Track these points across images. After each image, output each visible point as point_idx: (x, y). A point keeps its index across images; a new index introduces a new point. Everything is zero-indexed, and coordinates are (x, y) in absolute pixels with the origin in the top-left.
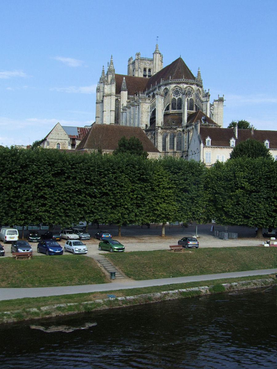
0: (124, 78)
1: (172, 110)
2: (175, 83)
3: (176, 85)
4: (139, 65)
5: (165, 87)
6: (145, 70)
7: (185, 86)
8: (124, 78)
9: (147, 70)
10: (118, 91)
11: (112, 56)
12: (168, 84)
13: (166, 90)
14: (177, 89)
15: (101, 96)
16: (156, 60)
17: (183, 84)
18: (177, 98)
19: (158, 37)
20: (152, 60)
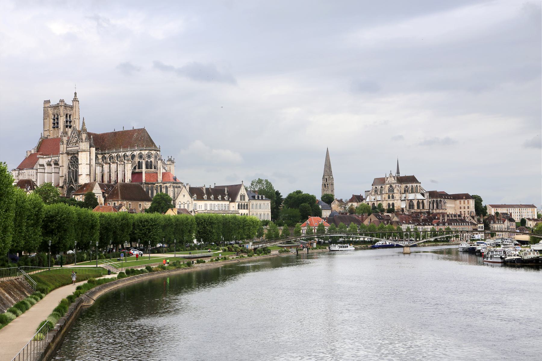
0: (92, 137)
1: (147, 170)
2: (148, 150)
4: (64, 111)
5: (140, 152)
6: (67, 115)
7: (155, 152)
8: (92, 137)
9: (68, 116)
10: (90, 147)
13: (141, 154)
14: (149, 154)
16: (76, 107)
17: (154, 151)
18: (149, 161)
20: (72, 107)
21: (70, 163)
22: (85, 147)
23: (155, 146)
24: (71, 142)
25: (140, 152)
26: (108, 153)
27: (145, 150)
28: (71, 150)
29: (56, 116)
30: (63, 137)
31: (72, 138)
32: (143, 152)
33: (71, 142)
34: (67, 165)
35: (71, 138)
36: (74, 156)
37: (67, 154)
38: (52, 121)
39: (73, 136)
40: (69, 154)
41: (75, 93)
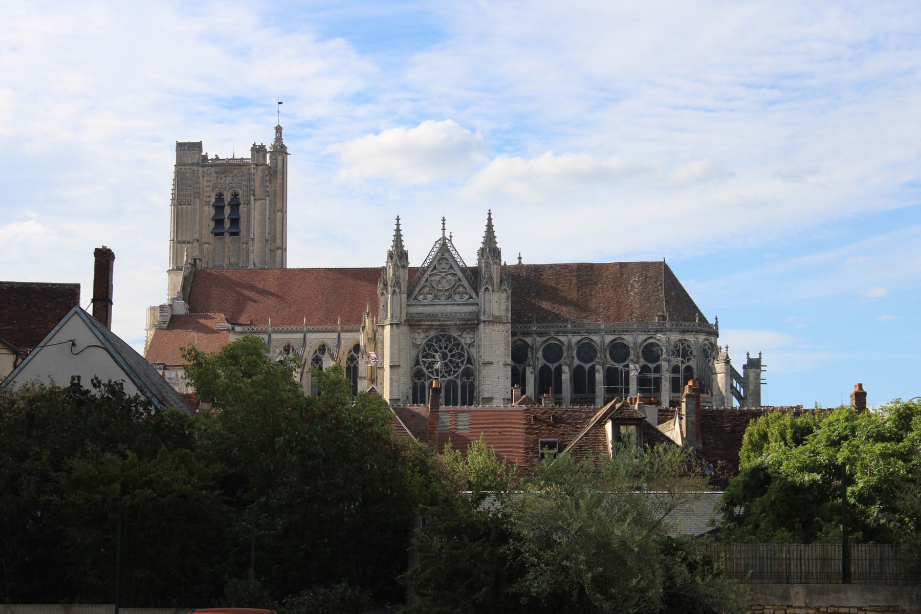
3: (705, 337)
5: (679, 337)
11: (490, 214)
12: (692, 331)
14: (705, 345)
15: (402, 305)
19: (280, 103)
21: (420, 358)
22: (499, 308)
23: (703, 319)
24: (423, 288)
25: (679, 337)
26: (540, 334)
27: (697, 332)
28: (429, 315)
29: (228, 198)
30: (400, 268)
31: (430, 276)
32: (689, 337)
33: (423, 288)
34: (411, 363)
35: (426, 276)
36: (443, 336)
37: (410, 325)
38: (210, 211)
39: (435, 268)
40: (421, 325)
41: (279, 129)
